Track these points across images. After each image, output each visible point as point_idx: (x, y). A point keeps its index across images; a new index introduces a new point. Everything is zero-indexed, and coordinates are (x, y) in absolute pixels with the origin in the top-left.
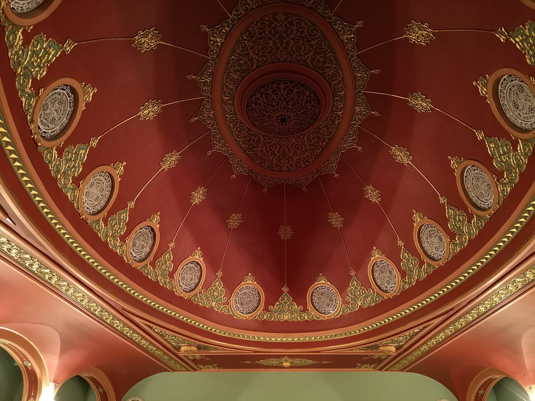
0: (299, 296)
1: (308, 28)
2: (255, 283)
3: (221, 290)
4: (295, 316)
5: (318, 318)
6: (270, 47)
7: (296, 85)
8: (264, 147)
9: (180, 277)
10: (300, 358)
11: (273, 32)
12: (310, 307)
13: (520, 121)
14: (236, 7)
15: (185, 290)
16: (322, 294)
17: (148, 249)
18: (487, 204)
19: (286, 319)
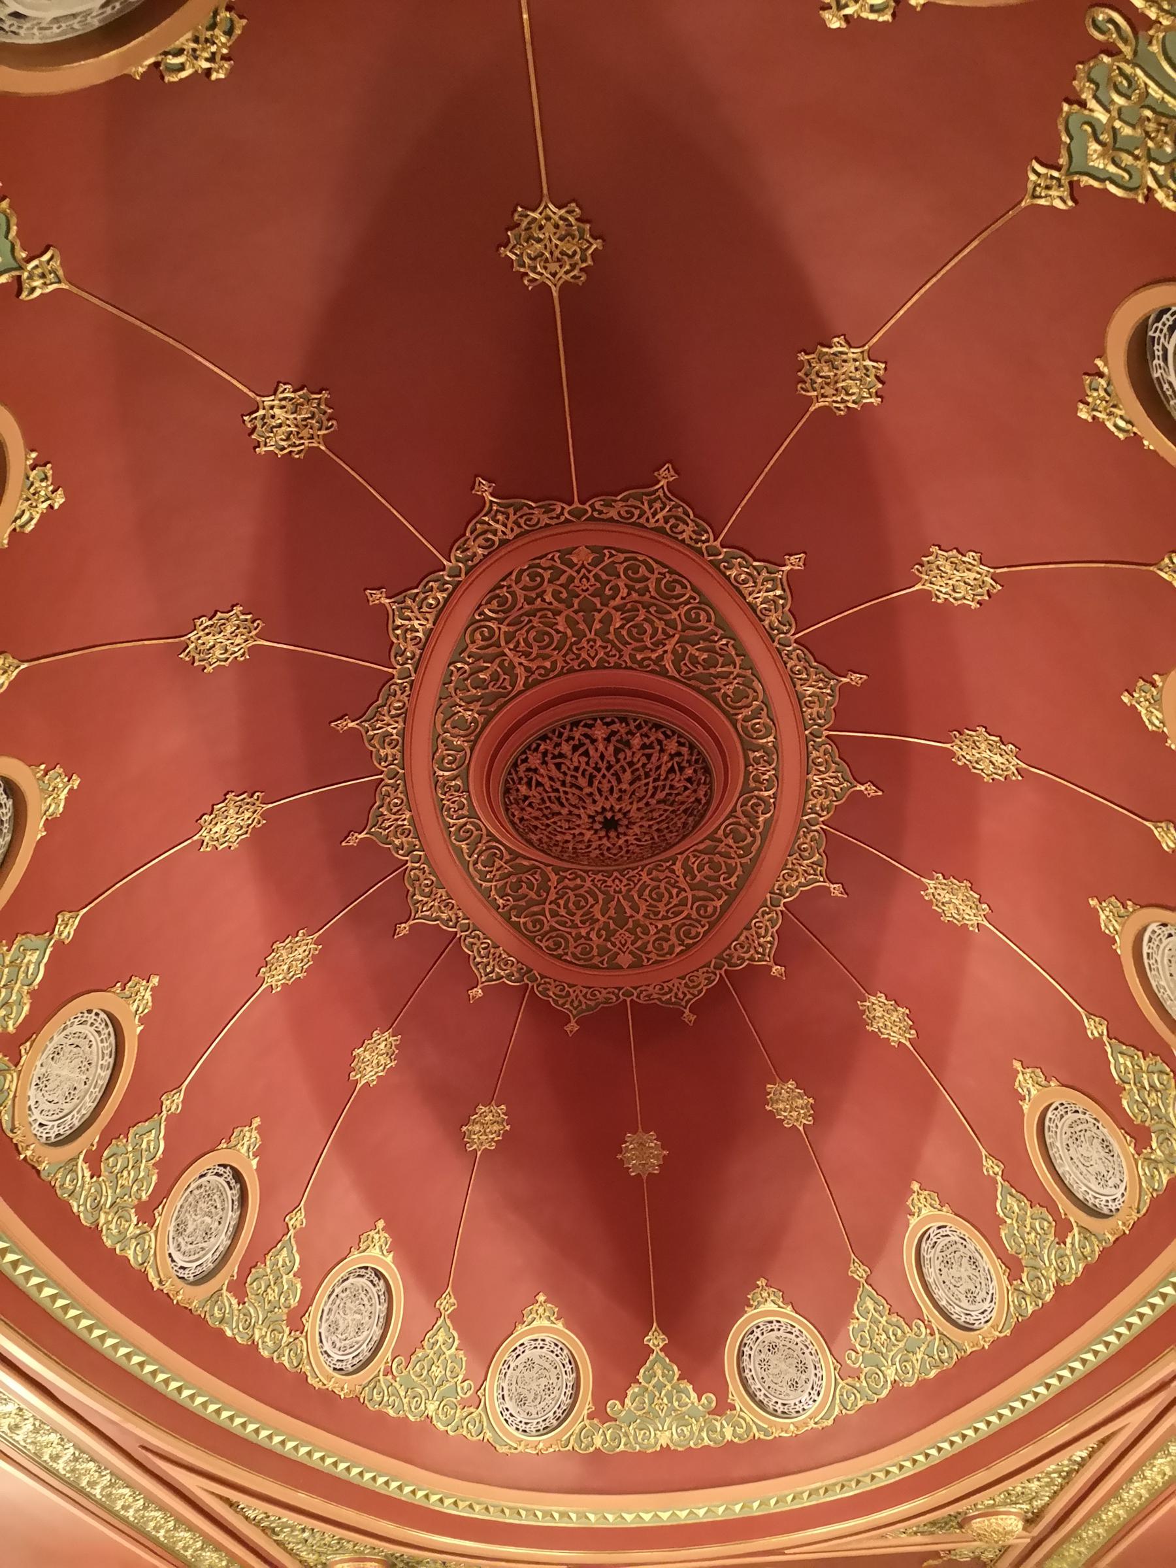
0: (699, 1359)
1: (659, 581)
2: (560, 1325)
3: (454, 1358)
6: (558, 632)
7: (639, 727)
8: (562, 902)
9: (325, 1325)
11: (564, 595)
14: (463, 539)
16: (772, 1348)
17: (223, 1241)
19: (664, 1440)
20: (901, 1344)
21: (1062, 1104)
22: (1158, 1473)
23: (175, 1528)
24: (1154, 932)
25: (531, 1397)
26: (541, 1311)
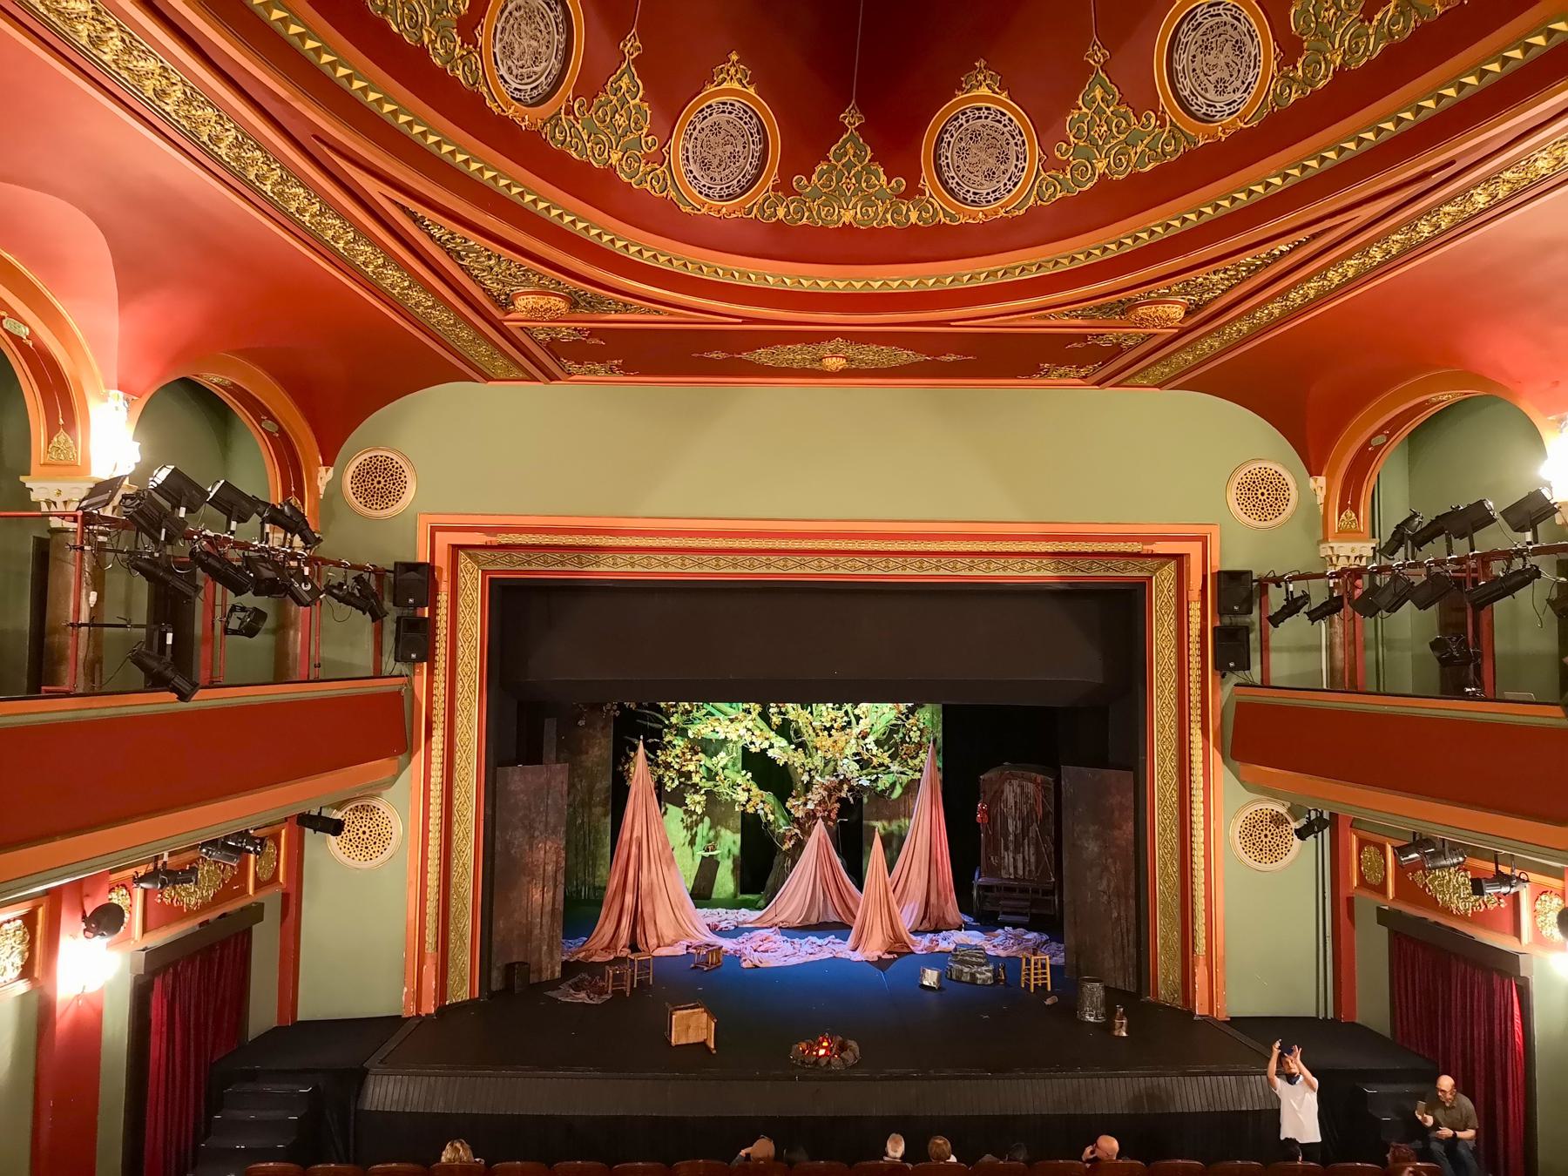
0: (897, 142)
2: (751, 91)
3: (638, 107)
4: (877, 213)
5: (953, 218)
9: (498, 45)
10: (879, 344)
12: (927, 181)
15: (517, 95)
16: (975, 136)
19: (847, 217)
20: (1122, 137)
23: (355, 241)
25: (716, 162)
26: (732, 71)
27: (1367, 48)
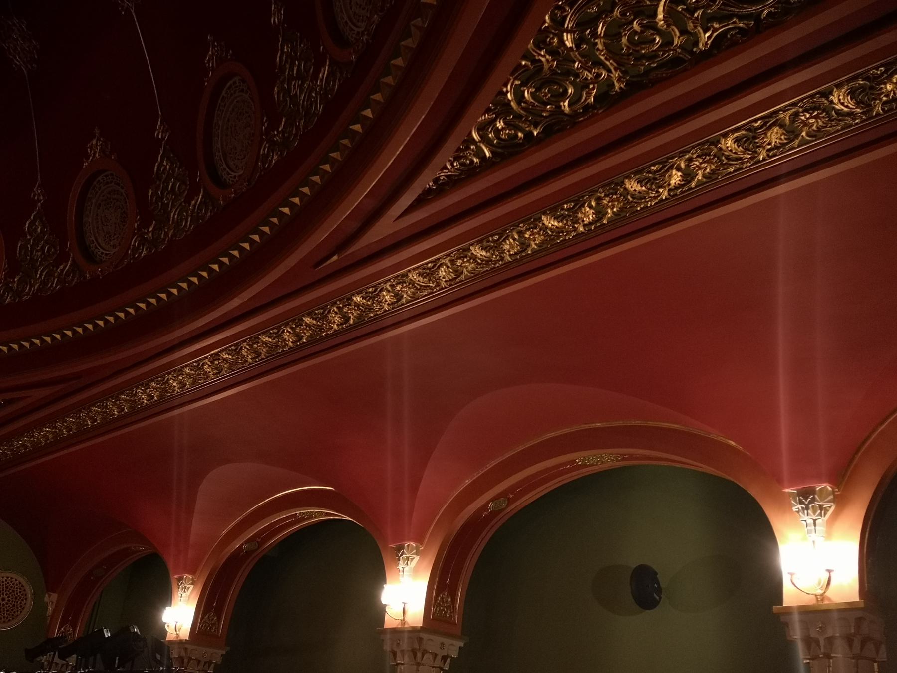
13: (346, 19)
18: (233, 174)
21: (112, 175)
22: (44, 436)
24: (235, 83)
27: (52, 286)
